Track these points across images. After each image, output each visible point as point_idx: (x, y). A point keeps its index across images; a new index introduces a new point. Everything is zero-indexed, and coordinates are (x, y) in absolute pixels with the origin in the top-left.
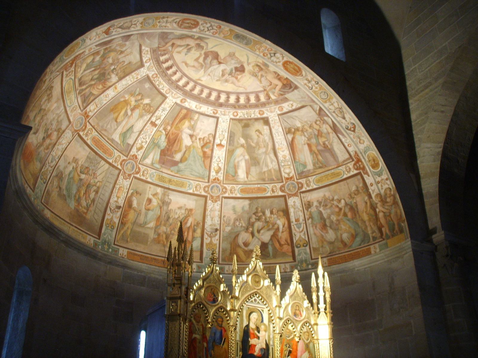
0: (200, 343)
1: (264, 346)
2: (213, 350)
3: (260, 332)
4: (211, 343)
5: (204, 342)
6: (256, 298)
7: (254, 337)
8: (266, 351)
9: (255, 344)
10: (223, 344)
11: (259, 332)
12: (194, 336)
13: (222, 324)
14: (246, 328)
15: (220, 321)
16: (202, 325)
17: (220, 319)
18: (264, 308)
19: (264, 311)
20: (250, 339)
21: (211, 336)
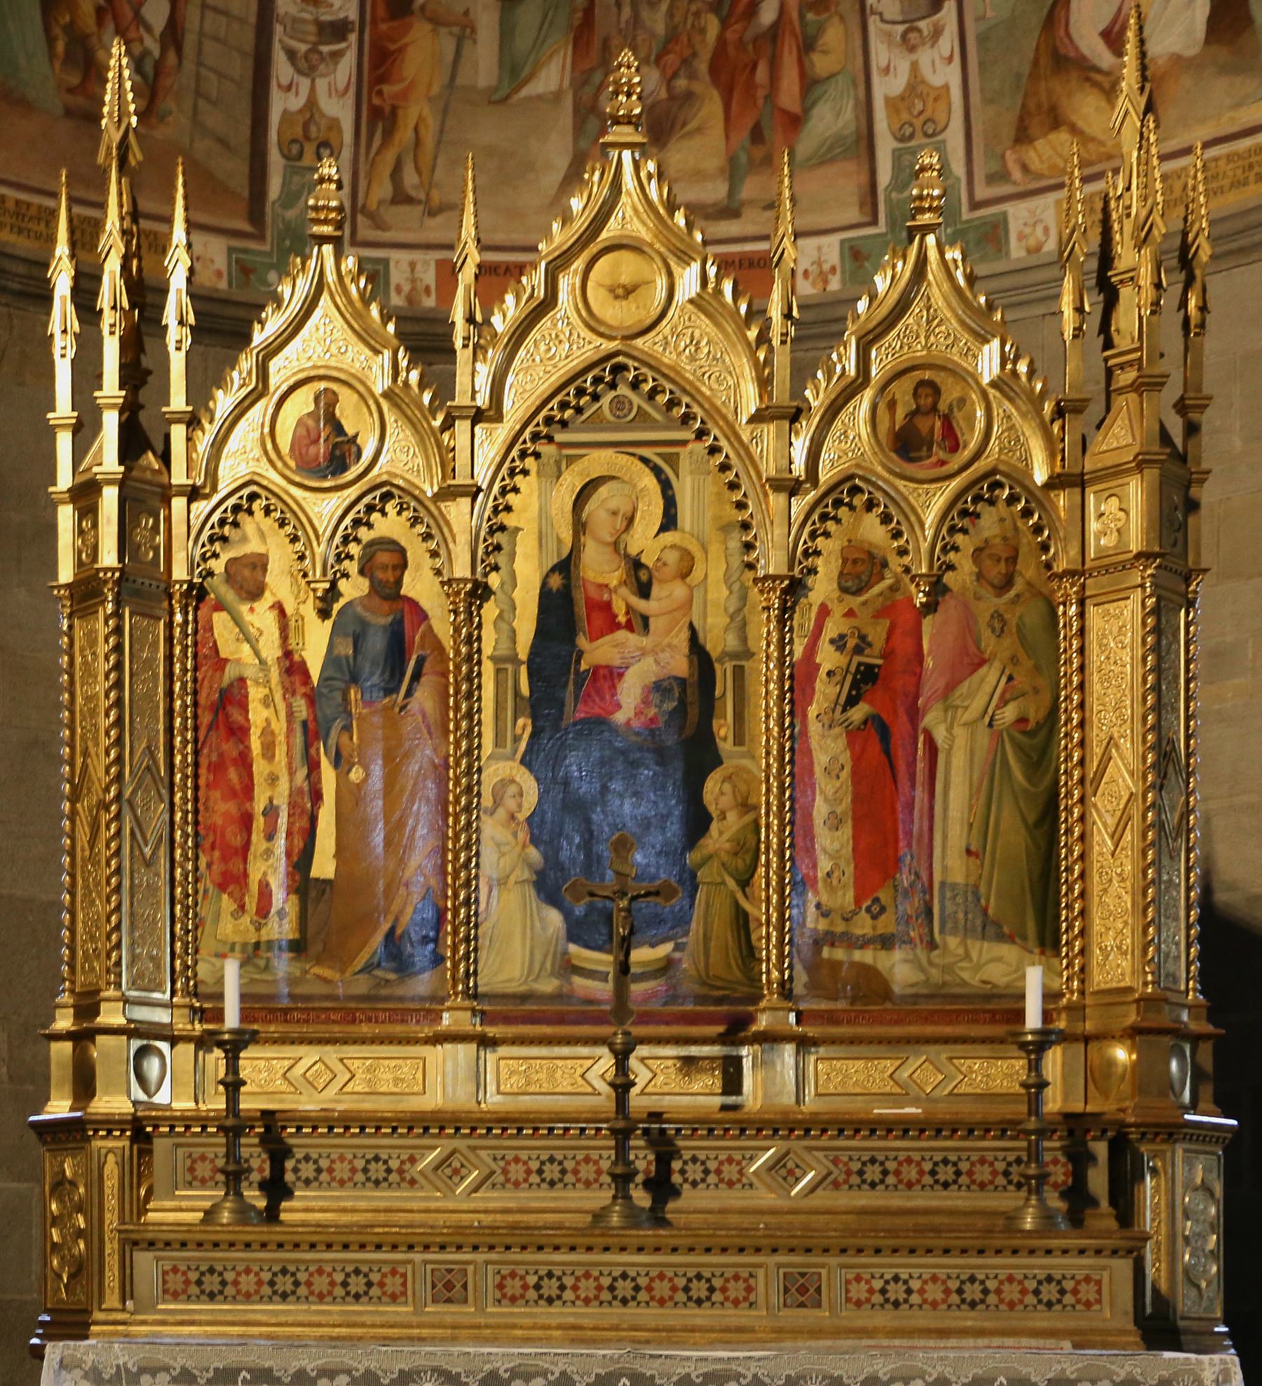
0: (267, 702)
1: (679, 664)
2: (347, 728)
3: (655, 590)
4: (338, 696)
5: (294, 693)
6: (623, 390)
7: (613, 626)
8: (693, 695)
9: (617, 662)
10: (409, 694)
11: (644, 591)
12: (230, 673)
13: (399, 582)
14: (556, 582)
15: (385, 567)
16: (279, 608)
17: (383, 558)
18: (684, 443)
19: (685, 464)
20: (582, 642)
21: (331, 660)
